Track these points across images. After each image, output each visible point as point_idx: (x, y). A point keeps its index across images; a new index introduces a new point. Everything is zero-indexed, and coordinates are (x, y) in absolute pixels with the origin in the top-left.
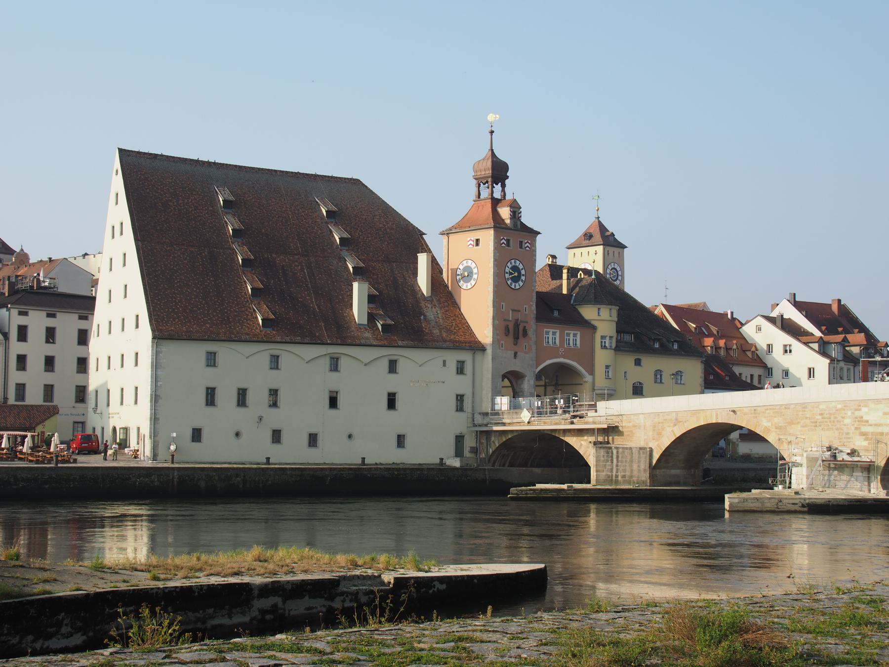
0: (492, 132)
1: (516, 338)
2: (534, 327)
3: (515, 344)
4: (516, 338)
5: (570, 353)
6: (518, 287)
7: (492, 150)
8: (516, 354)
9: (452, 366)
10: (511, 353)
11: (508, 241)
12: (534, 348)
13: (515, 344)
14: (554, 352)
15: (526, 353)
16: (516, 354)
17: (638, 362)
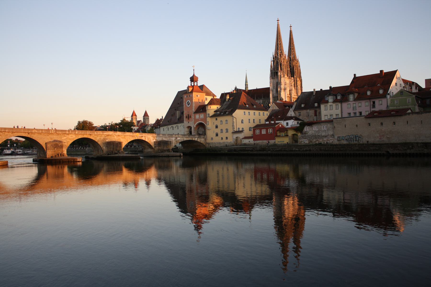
0: (194, 70)
1: (188, 118)
2: (193, 115)
3: (189, 120)
4: (188, 118)
5: (202, 120)
6: (188, 106)
7: (194, 74)
8: (189, 122)
9: (183, 126)
10: (188, 122)
11: (187, 96)
12: (193, 120)
13: (189, 120)
14: (198, 120)
15: (191, 121)
16: (189, 122)
17: (216, 119)
